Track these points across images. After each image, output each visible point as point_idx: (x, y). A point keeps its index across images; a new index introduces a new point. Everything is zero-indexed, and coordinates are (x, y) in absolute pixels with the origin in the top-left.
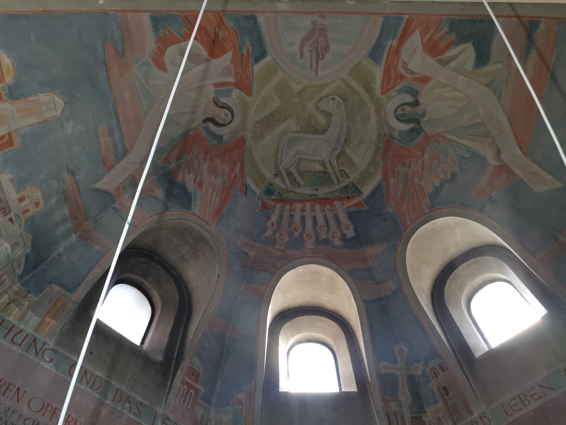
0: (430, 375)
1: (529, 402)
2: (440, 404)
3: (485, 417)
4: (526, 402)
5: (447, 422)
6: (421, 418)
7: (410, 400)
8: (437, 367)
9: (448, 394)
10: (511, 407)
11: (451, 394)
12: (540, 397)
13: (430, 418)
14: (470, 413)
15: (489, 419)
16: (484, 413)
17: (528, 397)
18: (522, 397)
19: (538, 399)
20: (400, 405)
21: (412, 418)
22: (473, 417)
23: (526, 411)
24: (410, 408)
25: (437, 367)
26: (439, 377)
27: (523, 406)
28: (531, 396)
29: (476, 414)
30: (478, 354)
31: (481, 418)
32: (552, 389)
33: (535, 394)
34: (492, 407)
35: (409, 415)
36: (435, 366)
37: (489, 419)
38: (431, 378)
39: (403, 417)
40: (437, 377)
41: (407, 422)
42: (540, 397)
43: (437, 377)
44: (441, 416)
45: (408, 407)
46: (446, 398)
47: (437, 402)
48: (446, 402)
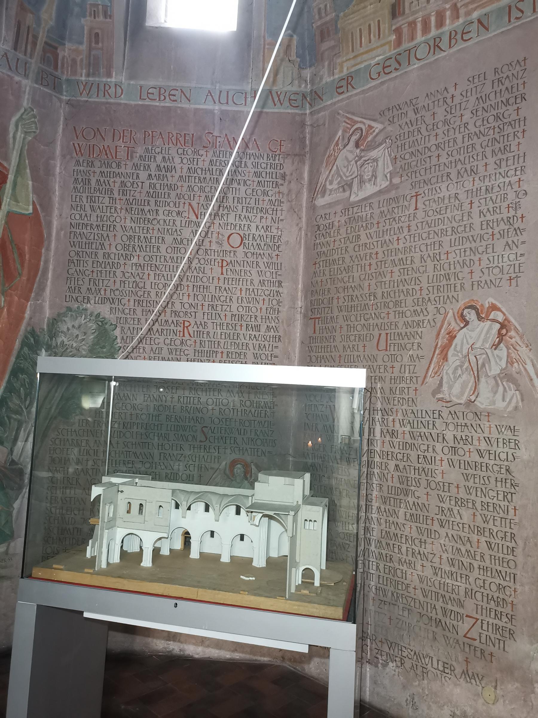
0: (88, 11)
1: (165, 99)
2: (84, 47)
3: (120, 87)
4: (162, 98)
5: (82, 69)
6: (56, 48)
7: (52, 23)
8: (100, 7)
9: (97, 42)
10: (148, 93)
11: (100, 45)
12: (176, 101)
13: (66, 54)
14: (109, 75)
15: (122, 90)
16: (121, 83)
17: (167, 94)
18: (162, 91)
19: (174, 101)
20: (38, 20)
21: (46, 43)
22: (109, 80)
23: (158, 104)
24: (48, 31)
25: (100, 7)
26: (97, 19)
27: (158, 99)
28: (169, 95)
29: (113, 80)
30: (150, 23)
31: (116, 85)
32: (189, 101)
33: (174, 95)
34: (132, 82)
35: (44, 39)
36: (99, 5)
37: (122, 90)
38: (88, 14)
39: (35, 37)
40: (95, 18)
41: (38, 44)
42: (176, 101)
43: (95, 18)
44: (78, 59)
45: (46, 29)
46: (93, 45)
47: (81, 43)
48: (90, 49)
